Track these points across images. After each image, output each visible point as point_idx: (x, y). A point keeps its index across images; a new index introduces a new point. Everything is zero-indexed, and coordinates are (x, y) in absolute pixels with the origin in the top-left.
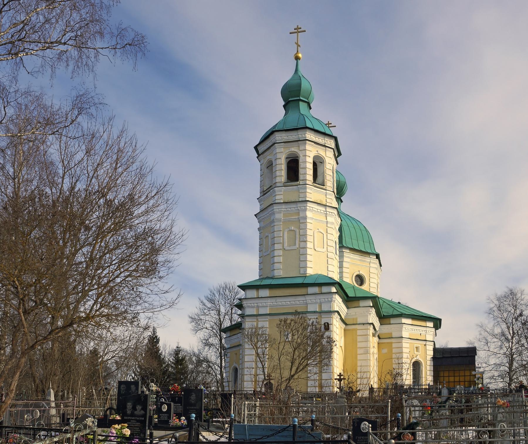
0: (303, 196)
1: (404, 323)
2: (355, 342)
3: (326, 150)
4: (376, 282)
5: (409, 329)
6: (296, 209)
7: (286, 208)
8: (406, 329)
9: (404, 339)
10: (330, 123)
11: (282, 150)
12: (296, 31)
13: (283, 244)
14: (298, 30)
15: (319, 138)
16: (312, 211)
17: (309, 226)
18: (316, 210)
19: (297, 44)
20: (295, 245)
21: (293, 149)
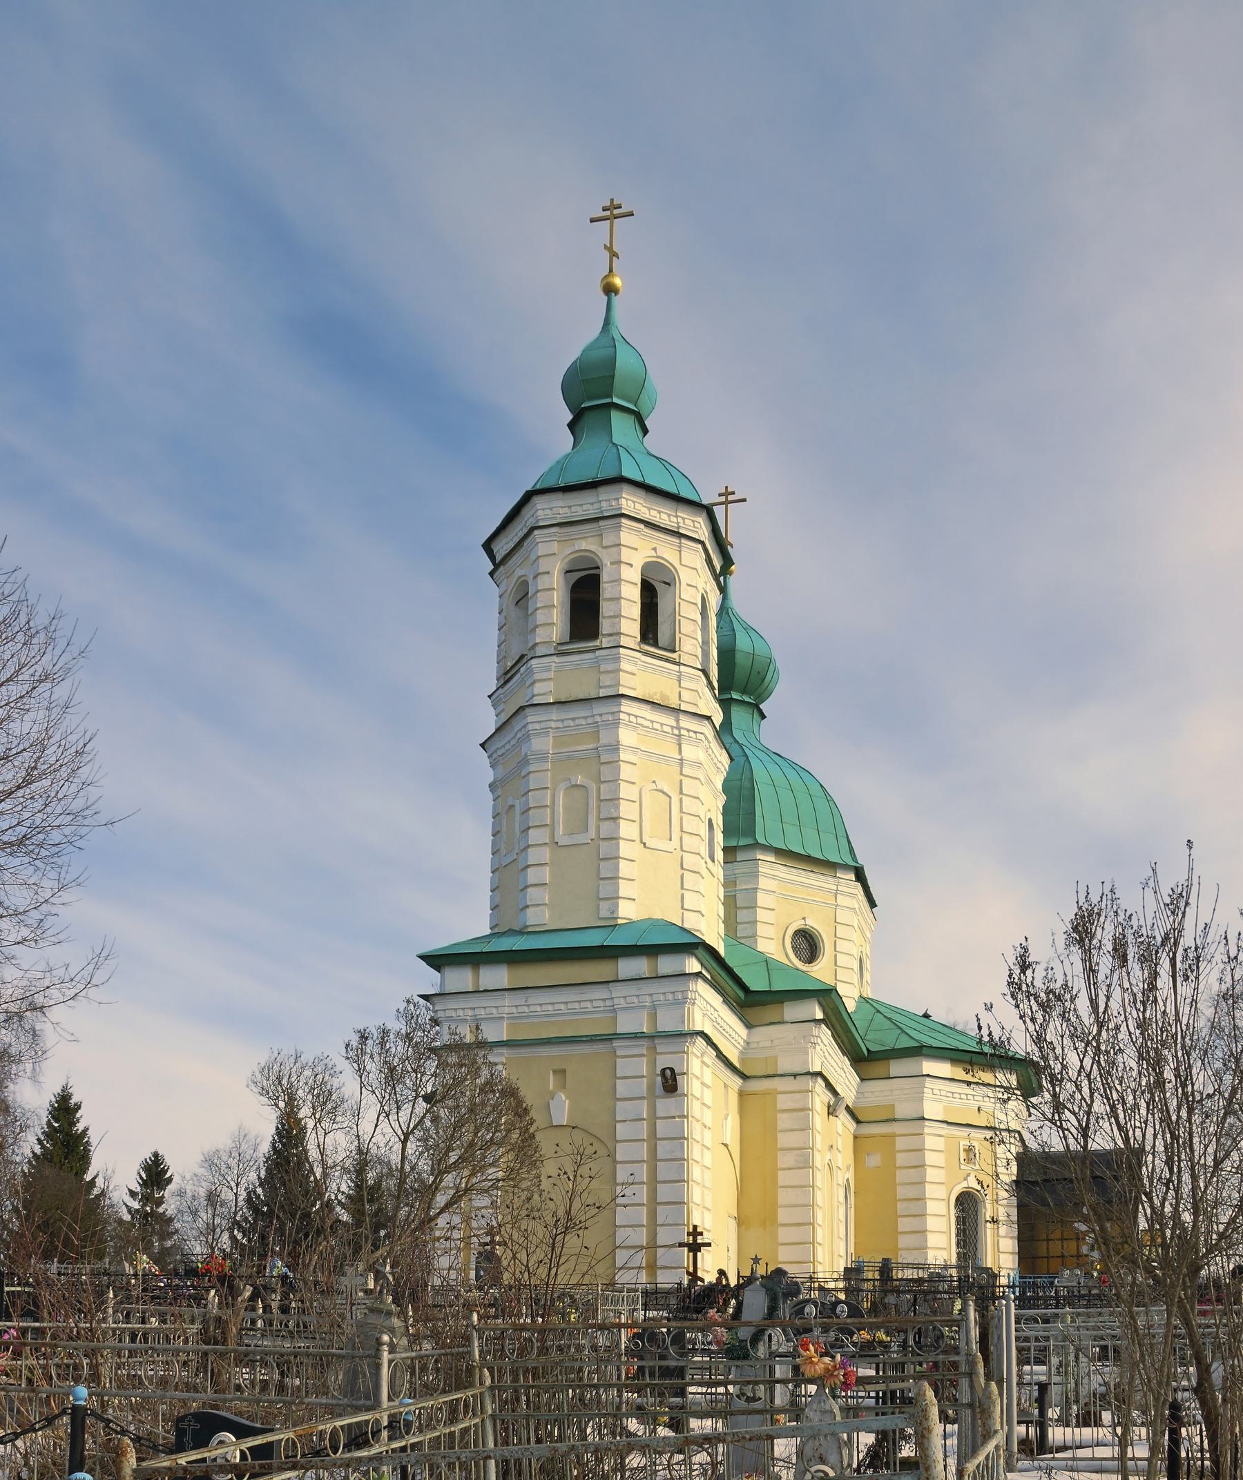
0: (608, 683)
1: (928, 1076)
2: (771, 1130)
3: (680, 547)
4: (855, 952)
5: (944, 1093)
6: (590, 720)
7: (562, 721)
8: (935, 1092)
9: (927, 1123)
10: (729, 490)
11: (554, 547)
12: (608, 213)
14: (612, 213)
15: (660, 512)
17: (626, 772)
19: (609, 249)
21: (584, 545)
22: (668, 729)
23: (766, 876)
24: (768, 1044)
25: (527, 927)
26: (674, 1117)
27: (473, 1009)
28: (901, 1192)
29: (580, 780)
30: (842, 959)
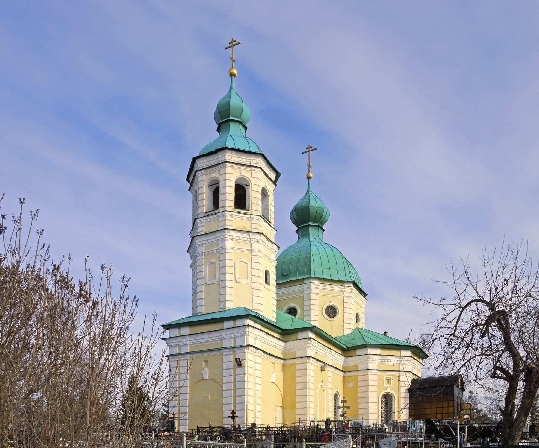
0: (222, 225)
1: (370, 354)
2: (294, 377)
3: (251, 171)
4: (352, 312)
6: (216, 239)
8: (373, 360)
9: (369, 371)
13: (205, 278)
15: (242, 159)
16: (232, 240)
17: (228, 256)
18: (238, 238)
20: (215, 278)
21: (214, 175)
22: (246, 239)
23: (314, 288)
24: (293, 347)
26: (241, 374)
28: (360, 395)
29: (213, 261)
30: (346, 315)
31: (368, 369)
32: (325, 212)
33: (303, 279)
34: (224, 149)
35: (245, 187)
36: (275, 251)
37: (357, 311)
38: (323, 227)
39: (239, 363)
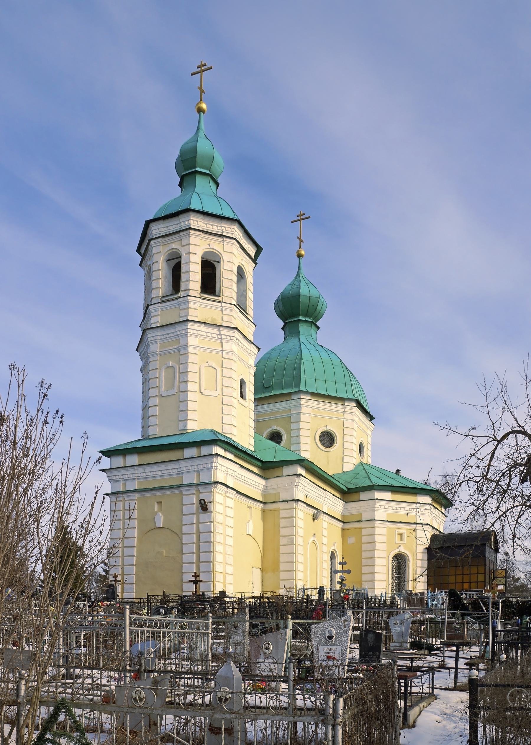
0: (184, 315)
1: (377, 499)
2: (277, 527)
3: (223, 242)
5: (386, 507)
6: (175, 334)
8: (382, 507)
9: (376, 522)
11: (161, 248)
13: (159, 387)
15: (212, 225)
16: (197, 335)
17: (191, 358)
18: (205, 334)
21: (173, 246)
22: (215, 336)
24: (275, 487)
25: (149, 436)
26: (207, 522)
27: (122, 475)
28: (364, 555)
29: (171, 363)
30: (346, 445)
31: (374, 520)
32: (320, 303)
33: (290, 394)
34: (188, 210)
35: (215, 264)
36: (253, 354)
37: (361, 439)
38: (318, 324)
39: (204, 507)
